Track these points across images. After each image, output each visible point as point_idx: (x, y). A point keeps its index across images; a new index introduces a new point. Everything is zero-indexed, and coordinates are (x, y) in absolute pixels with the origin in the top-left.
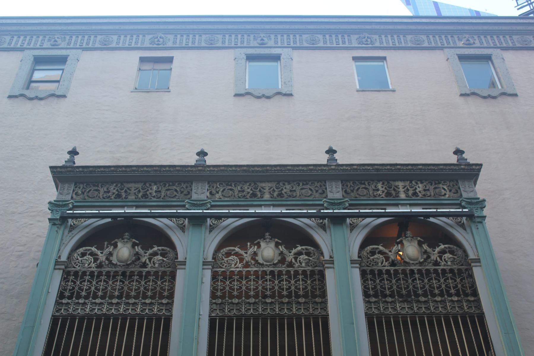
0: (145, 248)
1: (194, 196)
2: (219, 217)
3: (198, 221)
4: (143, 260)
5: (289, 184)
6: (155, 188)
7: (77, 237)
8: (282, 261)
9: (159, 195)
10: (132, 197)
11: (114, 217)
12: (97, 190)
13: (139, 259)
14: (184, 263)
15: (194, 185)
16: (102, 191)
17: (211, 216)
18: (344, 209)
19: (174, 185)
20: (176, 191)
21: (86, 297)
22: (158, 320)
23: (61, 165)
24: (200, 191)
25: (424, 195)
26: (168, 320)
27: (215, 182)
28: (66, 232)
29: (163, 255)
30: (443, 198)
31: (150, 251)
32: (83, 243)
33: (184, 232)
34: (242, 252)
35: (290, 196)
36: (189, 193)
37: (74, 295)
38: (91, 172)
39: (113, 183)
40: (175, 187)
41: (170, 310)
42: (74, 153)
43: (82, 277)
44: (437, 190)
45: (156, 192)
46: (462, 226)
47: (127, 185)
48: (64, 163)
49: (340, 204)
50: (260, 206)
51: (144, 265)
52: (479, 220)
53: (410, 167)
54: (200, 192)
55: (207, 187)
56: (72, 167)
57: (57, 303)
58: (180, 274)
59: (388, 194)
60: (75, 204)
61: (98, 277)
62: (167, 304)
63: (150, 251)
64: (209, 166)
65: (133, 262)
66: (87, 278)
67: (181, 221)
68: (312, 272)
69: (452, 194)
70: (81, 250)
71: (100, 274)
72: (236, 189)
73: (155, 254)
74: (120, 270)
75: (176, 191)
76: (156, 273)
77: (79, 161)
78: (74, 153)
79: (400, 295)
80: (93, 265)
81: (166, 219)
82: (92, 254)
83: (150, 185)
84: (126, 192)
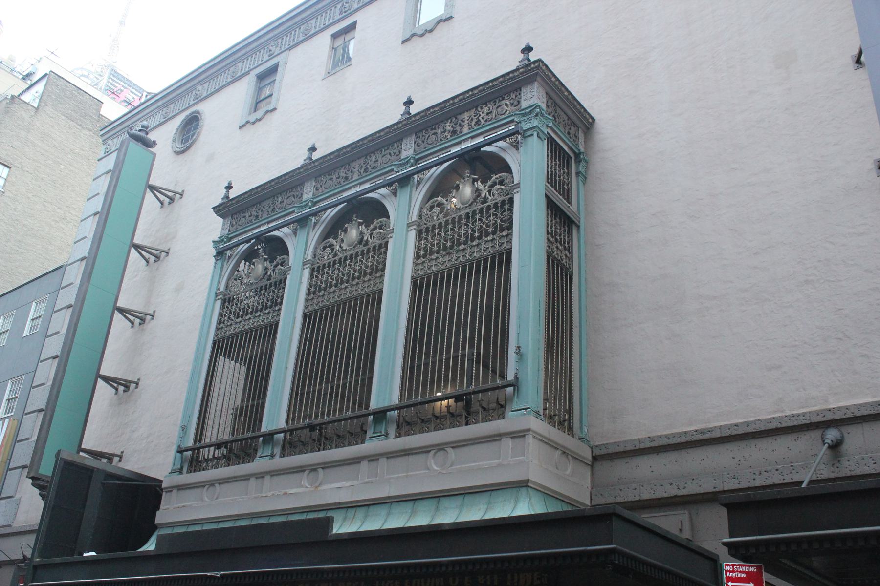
0: (484, 182)
1: (404, 155)
2: (315, 214)
3: (302, 222)
4: (483, 195)
5: (487, 105)
6: (486, 110)
7: (319, 230)
8: (361, 241)
9: (490, 117)
10: (466, 130)
11: (349, 200)
12: (435, 134)
13: (479, 195)
14: (518, 186)
15: (523, 90)
16: (334, 177)
17: (418, 172)
18: (412, 166)
19: (503, 99)
20: (506, 105)
21: (480, 238)
22: (501, 255)
23: (515, 68)
24: (529, 95)
25: (486, 121)
26: (509, 253)
27: (320, 176)
28: (414, 189)
29: (501, 183)
30: (503, 116)
31: (489, 183)
32: (433, 193)
33: (517, 149)
34: (444, 201)
35: (486, 121)
36: (519, 102)
37: (428, 252)
38: (441, 109)
39: (447, 120)
40: (504, 101)
41: (510, 242)
42: (409, 102)
43: (502, 207)
44: (499, 109)
45: (488, 114)
46: (516, 146)
47: (460, 117)
48: (518, 64)
49: (407, 162)
50: (350, 188)
51: (485, 200)
52: (529, 133)
53: (501, 79)
54: (408, 149)
55: (314, 183)
56: (410, 118)
57: (416, 264)
58: (517, 199)
59: (454, 132)
60: (417, 157)
61: (502, 207)
62: (507, 236)
63: (489, 183)
64: (415, 115)
65: (475, 200)
66: (492, 211)
67: (513, 138)
68: (503, 202)
69: (513, 108)
70: (430, 203)
71: (447, 222)
72: (439, 132)
73: (494, 184)
74: (463, 213)
75: (506, 105)
76: (496, 205)
77: (414, 110)
78: (229, 187)
79: (445, 249)
80: (441, 216)
81: (501, 142)
82: (440, 205)
83: (481, 108)
84: (460, 125)
